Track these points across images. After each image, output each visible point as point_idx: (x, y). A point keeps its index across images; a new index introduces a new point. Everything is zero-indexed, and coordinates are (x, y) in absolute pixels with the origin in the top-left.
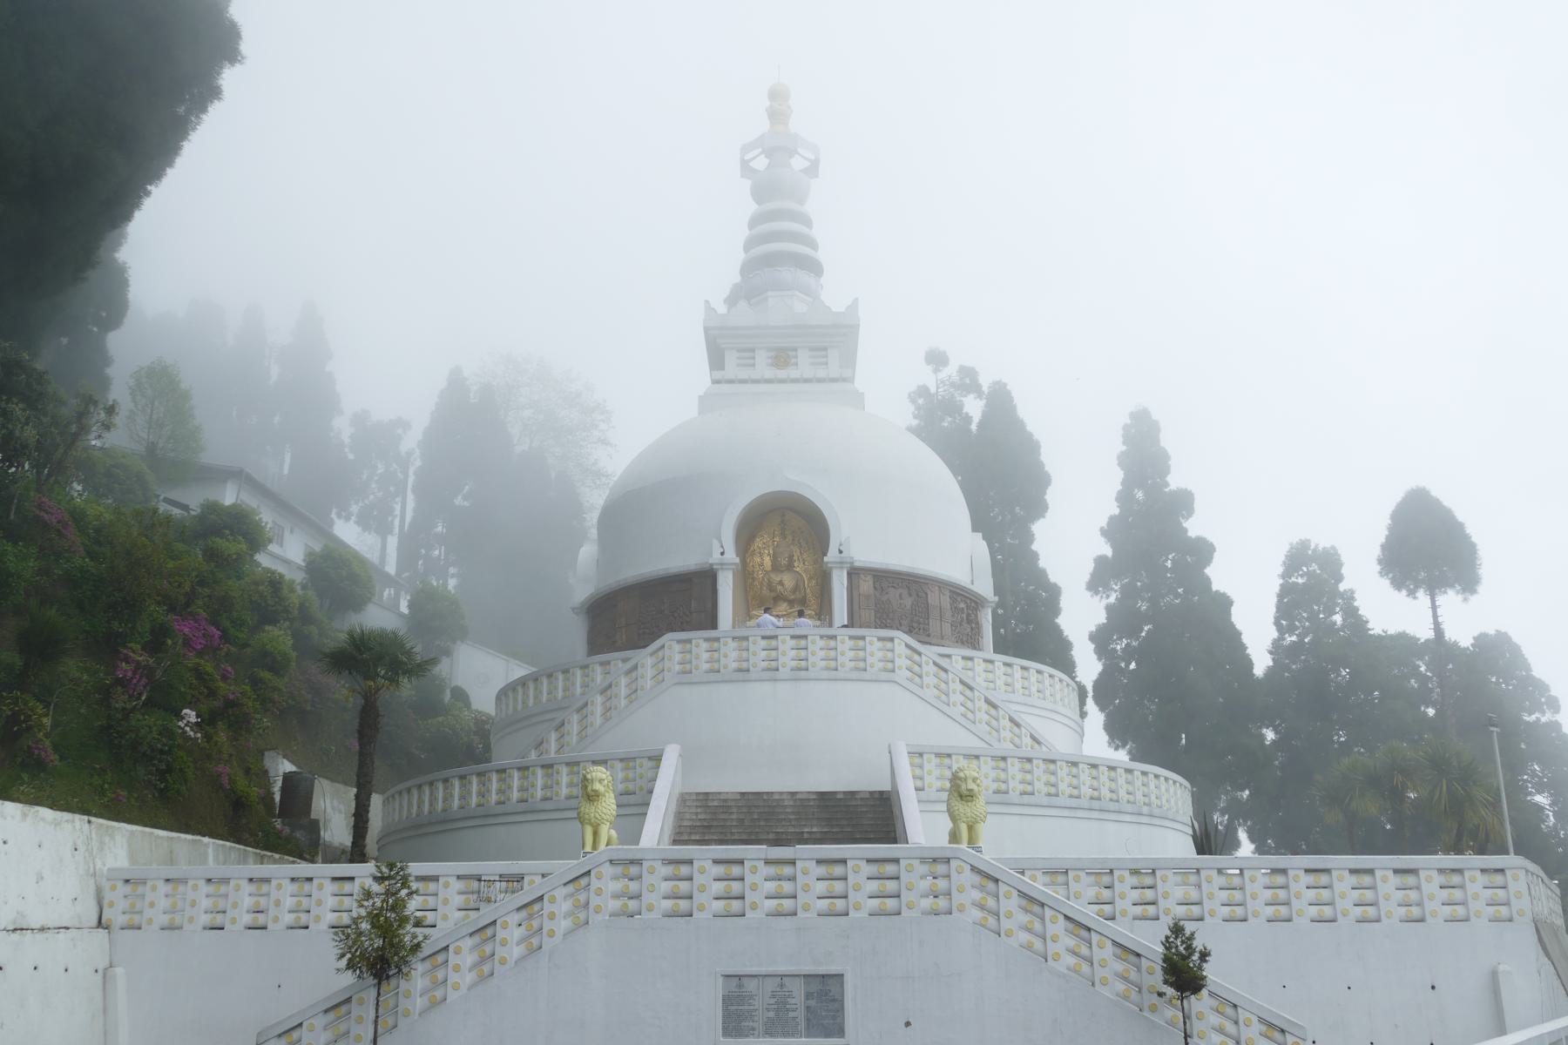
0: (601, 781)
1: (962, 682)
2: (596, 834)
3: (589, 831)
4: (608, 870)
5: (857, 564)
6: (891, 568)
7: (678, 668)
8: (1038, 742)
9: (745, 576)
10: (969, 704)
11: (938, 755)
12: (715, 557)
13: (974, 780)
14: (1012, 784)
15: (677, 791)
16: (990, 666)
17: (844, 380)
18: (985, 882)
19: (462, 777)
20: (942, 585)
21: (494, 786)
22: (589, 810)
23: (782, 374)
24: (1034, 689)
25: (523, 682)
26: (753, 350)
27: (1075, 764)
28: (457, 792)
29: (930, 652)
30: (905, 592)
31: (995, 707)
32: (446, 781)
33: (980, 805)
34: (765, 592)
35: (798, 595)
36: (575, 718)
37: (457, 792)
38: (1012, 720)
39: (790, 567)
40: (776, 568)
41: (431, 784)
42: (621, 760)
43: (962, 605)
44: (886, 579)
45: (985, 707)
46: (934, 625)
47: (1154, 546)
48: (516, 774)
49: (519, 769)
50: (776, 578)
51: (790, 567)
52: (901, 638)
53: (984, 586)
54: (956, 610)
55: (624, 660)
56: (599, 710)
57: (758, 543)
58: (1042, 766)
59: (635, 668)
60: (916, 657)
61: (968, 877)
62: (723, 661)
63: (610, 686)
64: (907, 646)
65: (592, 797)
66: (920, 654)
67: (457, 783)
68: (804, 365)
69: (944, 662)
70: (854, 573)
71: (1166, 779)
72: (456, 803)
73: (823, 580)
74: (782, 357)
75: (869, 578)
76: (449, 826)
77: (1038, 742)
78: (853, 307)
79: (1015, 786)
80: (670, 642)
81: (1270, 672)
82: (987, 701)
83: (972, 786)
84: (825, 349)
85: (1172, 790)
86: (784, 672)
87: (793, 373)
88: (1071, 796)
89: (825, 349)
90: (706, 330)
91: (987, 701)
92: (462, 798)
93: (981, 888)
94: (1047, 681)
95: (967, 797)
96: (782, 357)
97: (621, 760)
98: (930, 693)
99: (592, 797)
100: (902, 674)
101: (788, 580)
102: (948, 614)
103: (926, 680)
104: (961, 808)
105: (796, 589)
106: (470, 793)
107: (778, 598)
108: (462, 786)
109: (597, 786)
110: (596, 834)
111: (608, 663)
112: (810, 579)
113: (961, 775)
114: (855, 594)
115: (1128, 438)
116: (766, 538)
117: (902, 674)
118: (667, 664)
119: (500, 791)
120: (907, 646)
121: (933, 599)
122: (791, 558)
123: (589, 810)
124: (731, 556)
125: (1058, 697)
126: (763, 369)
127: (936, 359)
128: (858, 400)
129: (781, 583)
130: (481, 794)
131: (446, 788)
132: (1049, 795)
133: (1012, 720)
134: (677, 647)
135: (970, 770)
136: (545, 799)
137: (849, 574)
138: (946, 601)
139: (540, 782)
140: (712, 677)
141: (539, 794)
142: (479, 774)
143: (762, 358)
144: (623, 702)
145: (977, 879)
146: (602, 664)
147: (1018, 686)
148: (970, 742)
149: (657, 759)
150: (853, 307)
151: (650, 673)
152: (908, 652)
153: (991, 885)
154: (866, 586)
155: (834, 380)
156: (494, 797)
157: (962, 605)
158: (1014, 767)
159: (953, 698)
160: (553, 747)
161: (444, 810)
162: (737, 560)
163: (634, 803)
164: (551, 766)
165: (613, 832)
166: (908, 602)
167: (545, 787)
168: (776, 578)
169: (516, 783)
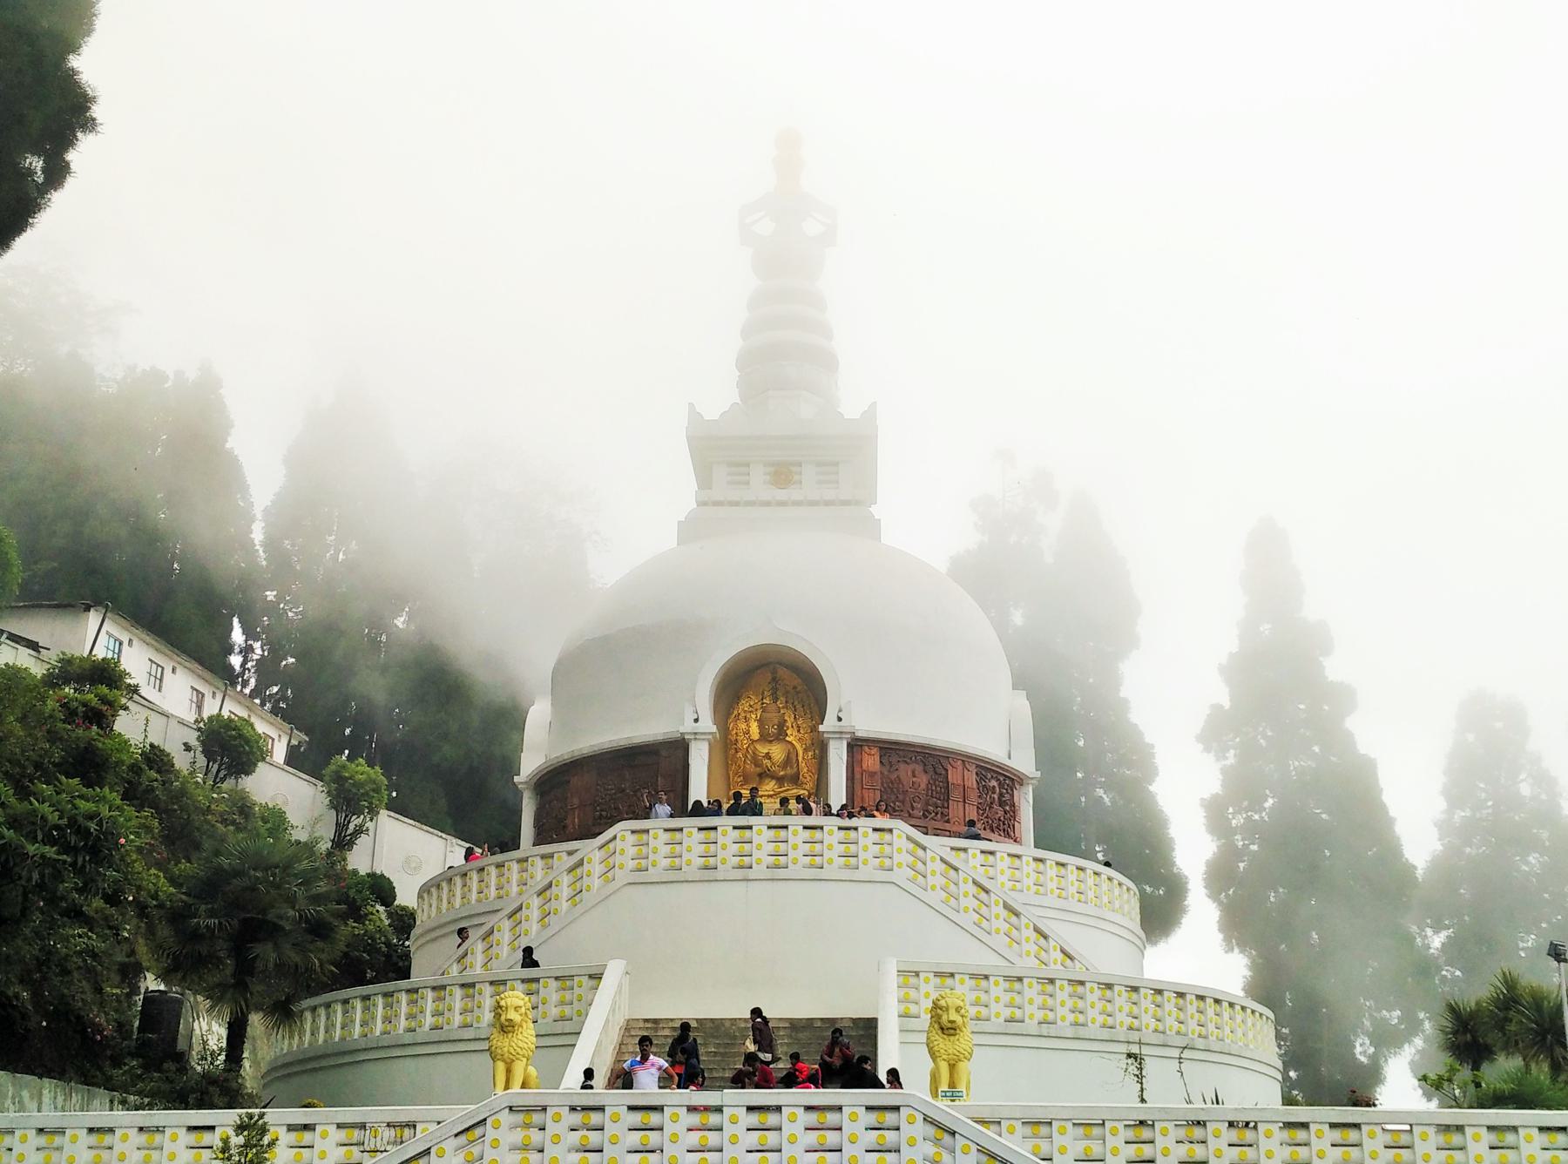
0: (517, 1008)
1: (975, 882)
2: (509, 1071)
3: (501, 1066)
4: (506, 1118)
5: (859, 734)
6: (902, 739)
7: (632, 864)
8: (1071, 958)
9: (726, 746)
10: (984, 910)
11: (938, 974)
12: (687, 727)
13: (958, 1009)
14: (1029, 1009)
15: (620, 1020)
16: (1017, 862)
17: (857, 503)
18: (940, 1134)
19: (366, 998)
20: (966, 759)
21: (404, 1008)
22: (503, 1044)
23: (781, 494)
24: (1072, 890)
25: (448, 877)
26: (748, 465)
27: (1135, 989)
28: (339, 1019)
29: (939, 845)
30: (919, 768)
31: (1017, 914)
32: (346, 1002)
33: (965, 1040)
34: (750, 768)
35: (789, 771)
36: (506, 924)
37: (339, 1019)
38: (1037, 930)
39: (780, 735)
40: (765, 738)
41: (328, 1006)
42: (557, 978)
43: (994, 783)
44: (891, 750)
45: (1004, 913)
46: (955, 810)
47: (1280, 695)
48: (430, 995)
49: (434, 988)
50: (762, 749)
51: (780, 735)
52: (901, 827)
53: (1023, 762)
54: (984, 789)
55: (570, 853)
56: (535, 914)
57: (744, 705)
58: (1068, 989)
59: (581, 863)
60: (920, 852)
61: (920, 1129)
62: (686, 857)
63: (550, 885)
64: (908, 838)
65: (506, 1028)
66: (924, 849)
67: (358, 1005)
69: (954, 858)
70: (857, 746)
71: (1243, 1008)
72: (357, 1031)
73: (820, 748)
74: (783, 475)
75: (875, 751)
76: (347, 1059)
77: (1071, 958)
78: (870, 414)
79: (1033, 1014)
80: (622, 828)
81: (1436, 865)
82: (1006, 906)
83: (953, 1016)
84: (836, 464)
85: (1259, 1024)
86: (759, 871)
87: (795, 494)
88: (1103, 1026)
89: (836, 464)
90: (690, 439)
91: (1006, 906)
92: (364, 1024)
93: (936, 1142)
94: (1091, 880)
95: (949, 1030)
96: (783, 475)
97: (557, 978)
98: (935, 897)
99: (506, 1028)
100: (902, 875)
101: (777, 752)
102: (973, 797)
103: (931, 880)
104: (941, 1043)
105: (787, 762)
106: (374, 1018)
108: (366, 1009)
109: (512, 1015)
110: (509, 1071)
111: (551, 856)
112: (806, 750)
113: (942, 1003)
114: (857, 770)
116: (754, 700)
117: (902, 875)
118: (618, 859)
119: (410, 1017)
120: (908, 838)
121: (954, 777)
122: (782, 726)
123: (503, 1044)
124: (708, 725)
125: (1105, 900)
126: (759, 486)
128: (872, 528)
129: (768, 756)
130: (387, 1020)
131: (345, 1012)
132: (1076, 1024)
133: (1037, 930)
134: (631, 838)
135: (961, 994)
136: (435, 1028)
137: (849, 745)
138: (971, 779)
139: (458, 1006)
140: (673, 876)
141: (457, 1019)
142: (386, 995)
143: (758, 476)
144: (565, 905)
145: (931, 1131)
146: (543, 857)
147: (1052, 885)
148: (984, 959)
149: (597, 977)
150: (870, 414)
151: (598, 869)
152: (912, 846)
153: (947, 1138)
154: (871, 761)
155: (846, 503)
156: (403, 1023)
157: (994, 783)
158: (1031, 990)
159: (964, 902)
160: (479, 959)
161: (343, 1039)
162: (714, 729)
163: (560, 1037)
164: (473, 985)
165: (532, 1070)
166: (923, 780)
167: (464, 1012)
168: (762, 749)
169: (430, 1006)
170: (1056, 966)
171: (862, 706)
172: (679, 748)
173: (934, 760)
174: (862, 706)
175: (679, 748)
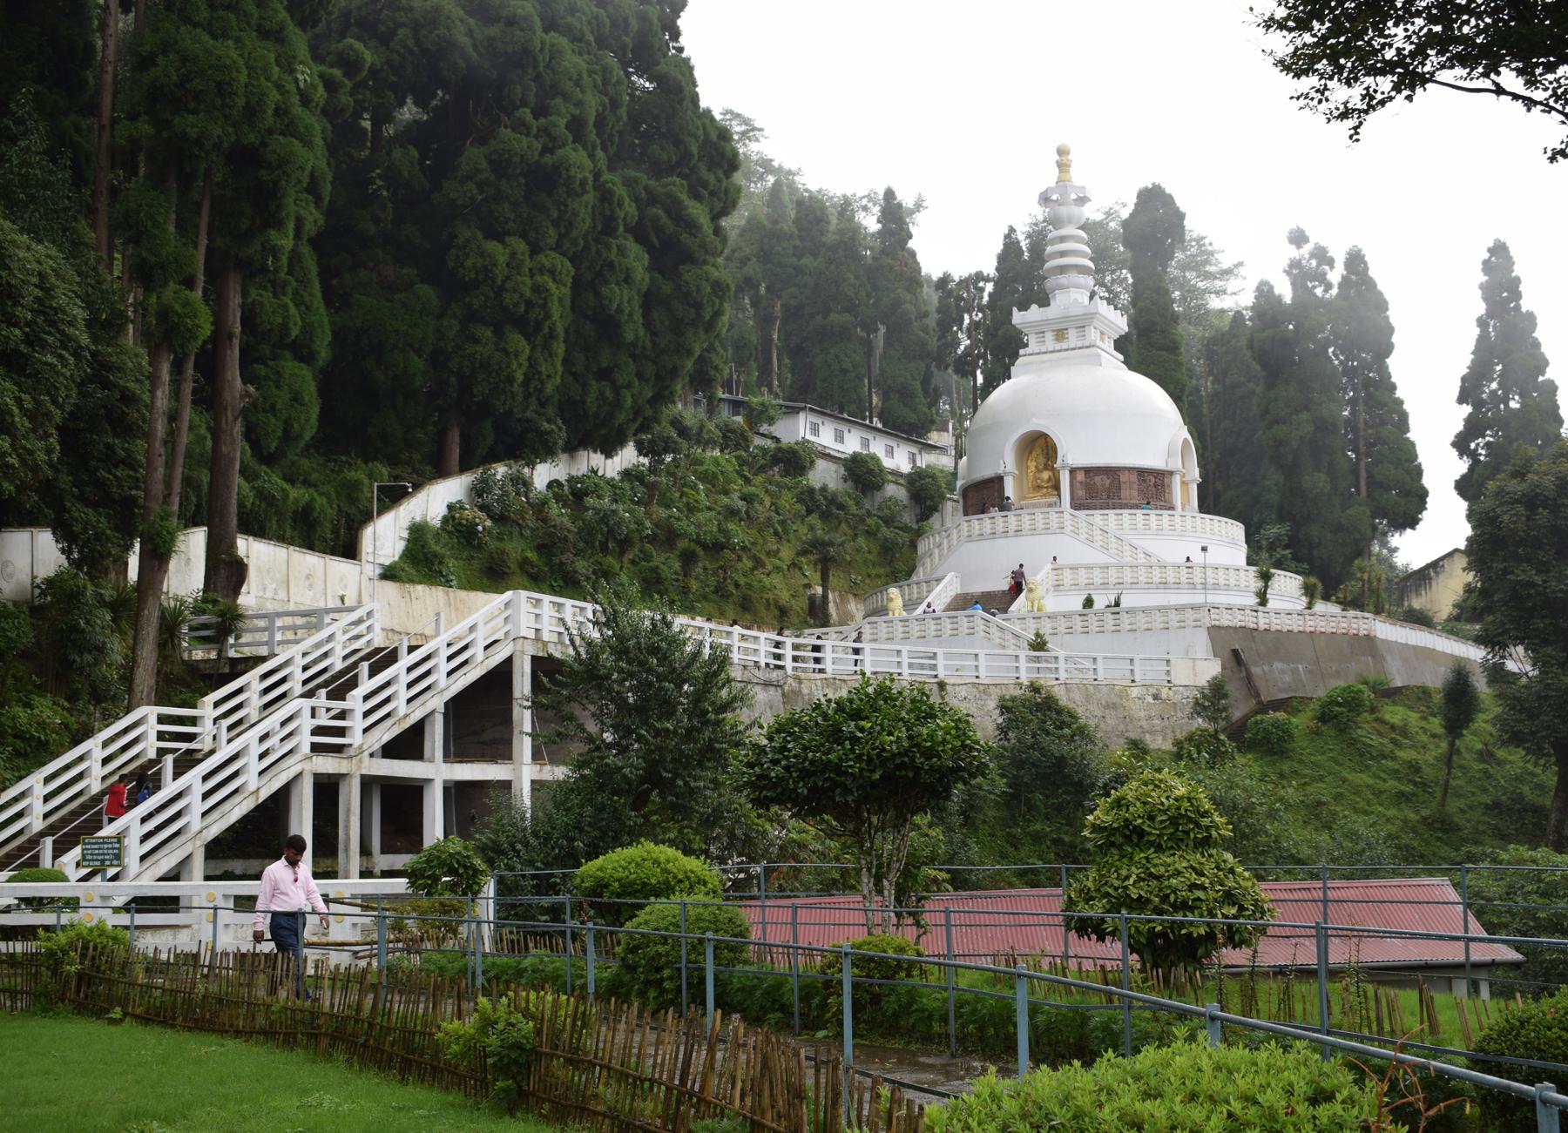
12: (1000, 471)
44: (1090, 471)
46: (1124, 493)
68: (1073, 338)
70: (1073, 471)
74: (1060, 335)
86: (1011, 533)
87: (1064, 345)
96: (1060, 335)
107: (1040, 487)
115: (1487, 266)
127: (1298, 238)
138: (1134, 477)
143: (1049, 337)
148: (1103, 559)
154: (1080, 476)
166: (1107, 482)
170: (1142, 559)
171: (1075, 452)
172: (999, 480)
173: (1111, 472)
174: (1075, 452)
175: (999, 480)
